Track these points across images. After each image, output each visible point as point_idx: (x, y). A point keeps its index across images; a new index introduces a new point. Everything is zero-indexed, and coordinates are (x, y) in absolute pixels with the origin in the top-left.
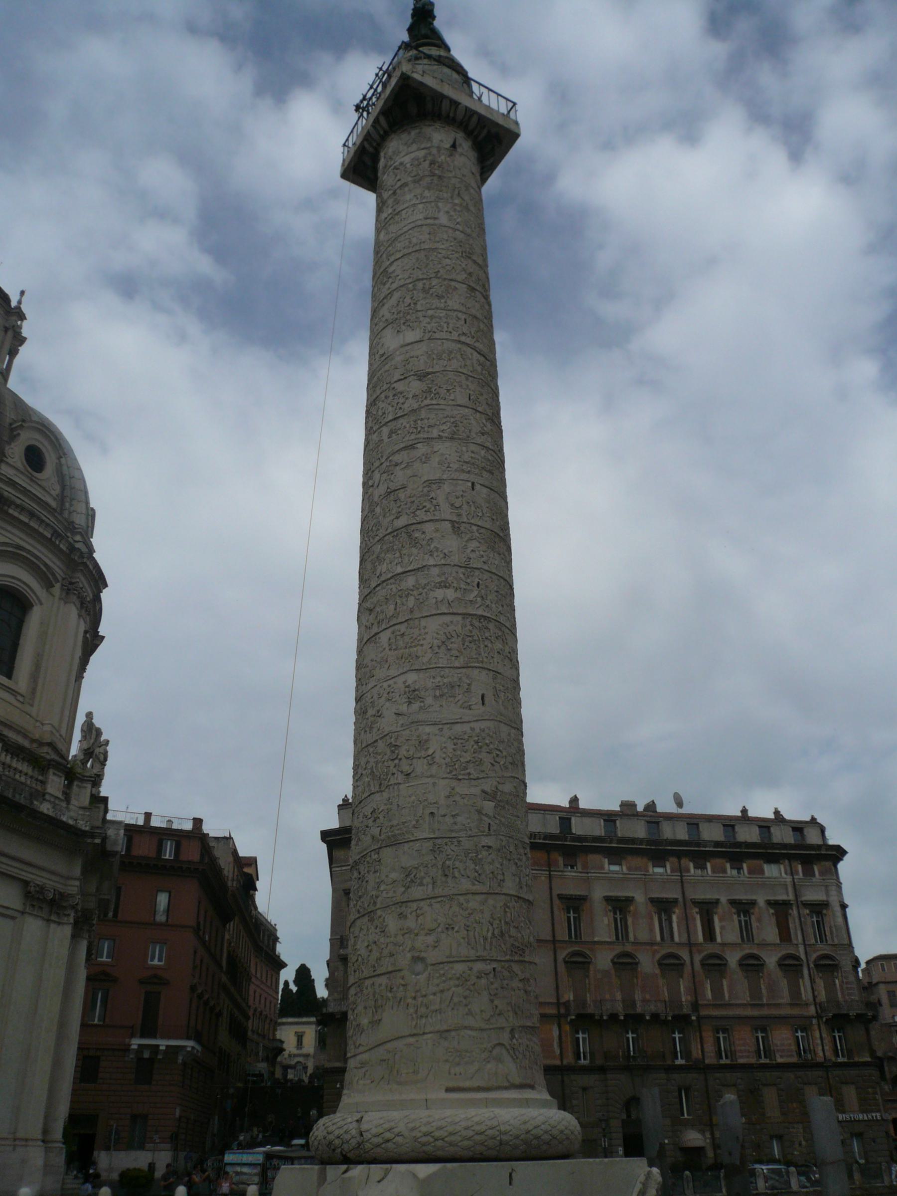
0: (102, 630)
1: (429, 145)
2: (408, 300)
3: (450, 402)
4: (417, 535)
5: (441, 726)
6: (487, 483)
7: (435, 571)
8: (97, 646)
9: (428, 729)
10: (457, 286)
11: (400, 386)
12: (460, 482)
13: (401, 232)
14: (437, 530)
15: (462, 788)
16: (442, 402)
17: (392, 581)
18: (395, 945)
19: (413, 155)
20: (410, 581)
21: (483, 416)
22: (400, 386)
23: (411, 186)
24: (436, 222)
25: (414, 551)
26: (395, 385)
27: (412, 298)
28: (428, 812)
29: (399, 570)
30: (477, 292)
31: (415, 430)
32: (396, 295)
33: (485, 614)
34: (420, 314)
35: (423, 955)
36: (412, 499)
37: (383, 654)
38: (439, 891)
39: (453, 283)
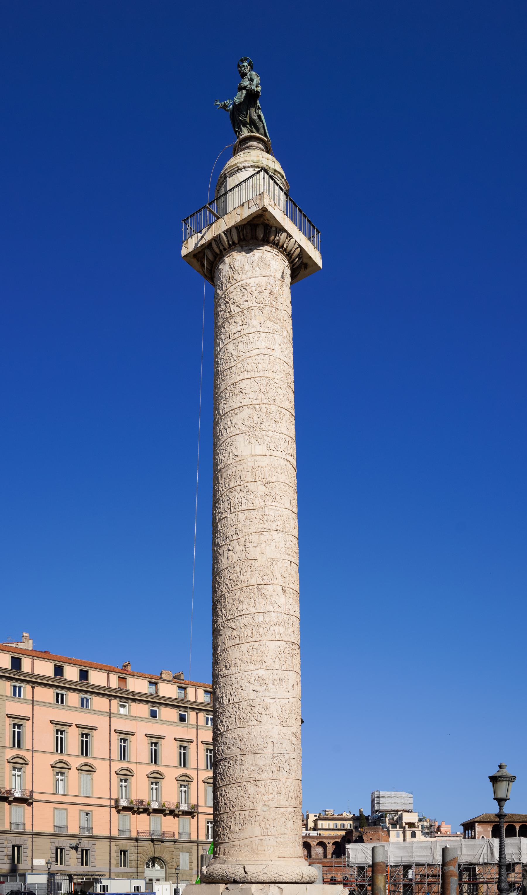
1: (268, 274)
3: (282, 506)
4: (264, 591)
5: (276, 700)
7: (274, 615)
9: (270, 700)
11: (251, 486)
13: (248, 354)
14: (274, 591)
15: (285, 730)
17: (249, 616)
18: (254, 798)
20: (260, 619)
22: (251, 486)
23: (257, 311)
24: (273, 353)
25: (264, 602)
26: (248, 484)
28: (270, 741)
29: (253, 610)
31: (262, 522)
32: (247, 411)
34: (264, 432)
35: (268, 804)
36: (261, 568)
37: (244, 657)
38: (275, 777)
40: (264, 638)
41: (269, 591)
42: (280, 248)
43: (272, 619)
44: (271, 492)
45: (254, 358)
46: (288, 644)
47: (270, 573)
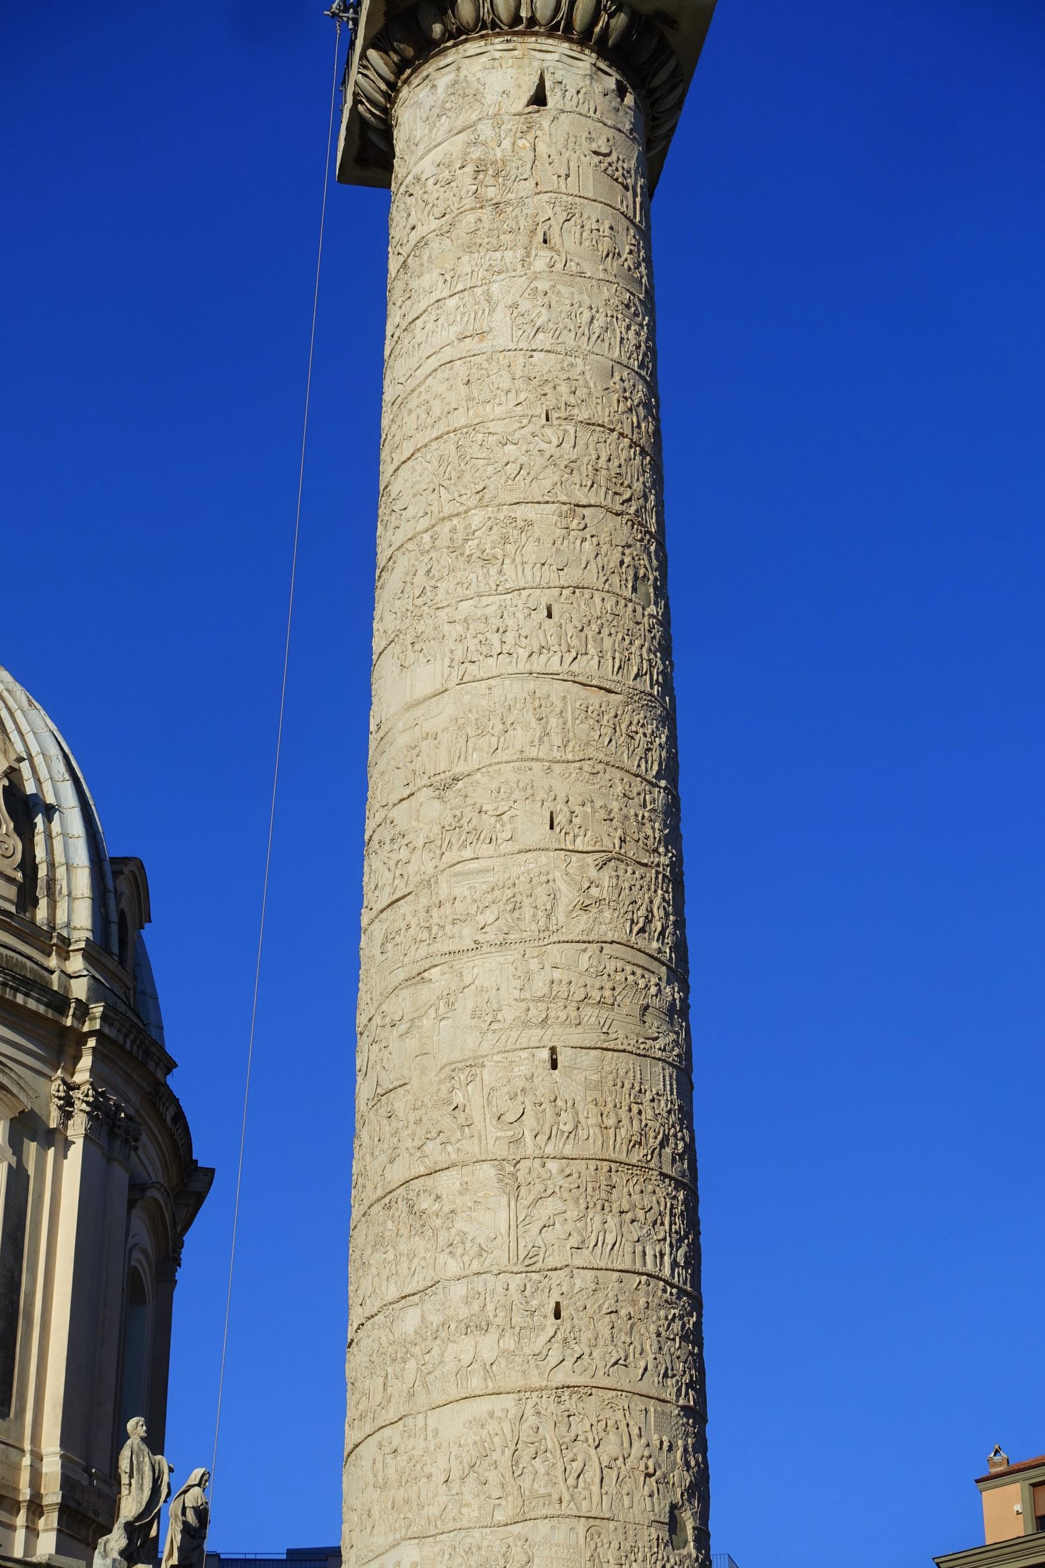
0: (202, 1156)
2: (420, 578)
3: (505, 848)
4: (425, 1203)
6: (591, 1039)
7: (459, 1290)
8: (200, 1199)
10: (531, 516)
12: (524, 1054)
16: (485, 849)
19: (436, 155)
20: (410, 1321)
21: (590, 859)
24: (485, 346)
25: (420, 1244)
27: (429, 571)
29: (392, 1292)
30: (586, 512)
31: (425, 935)
33: (573, 1381)
39: (520, 512)
40: (422, 1400)
41: (444, 1196)
42: (511, 26)
43: (451, 1312)
44: (458, 813)
45: (422, 389)
46: (531, 1403)
47: (446, 1122)
